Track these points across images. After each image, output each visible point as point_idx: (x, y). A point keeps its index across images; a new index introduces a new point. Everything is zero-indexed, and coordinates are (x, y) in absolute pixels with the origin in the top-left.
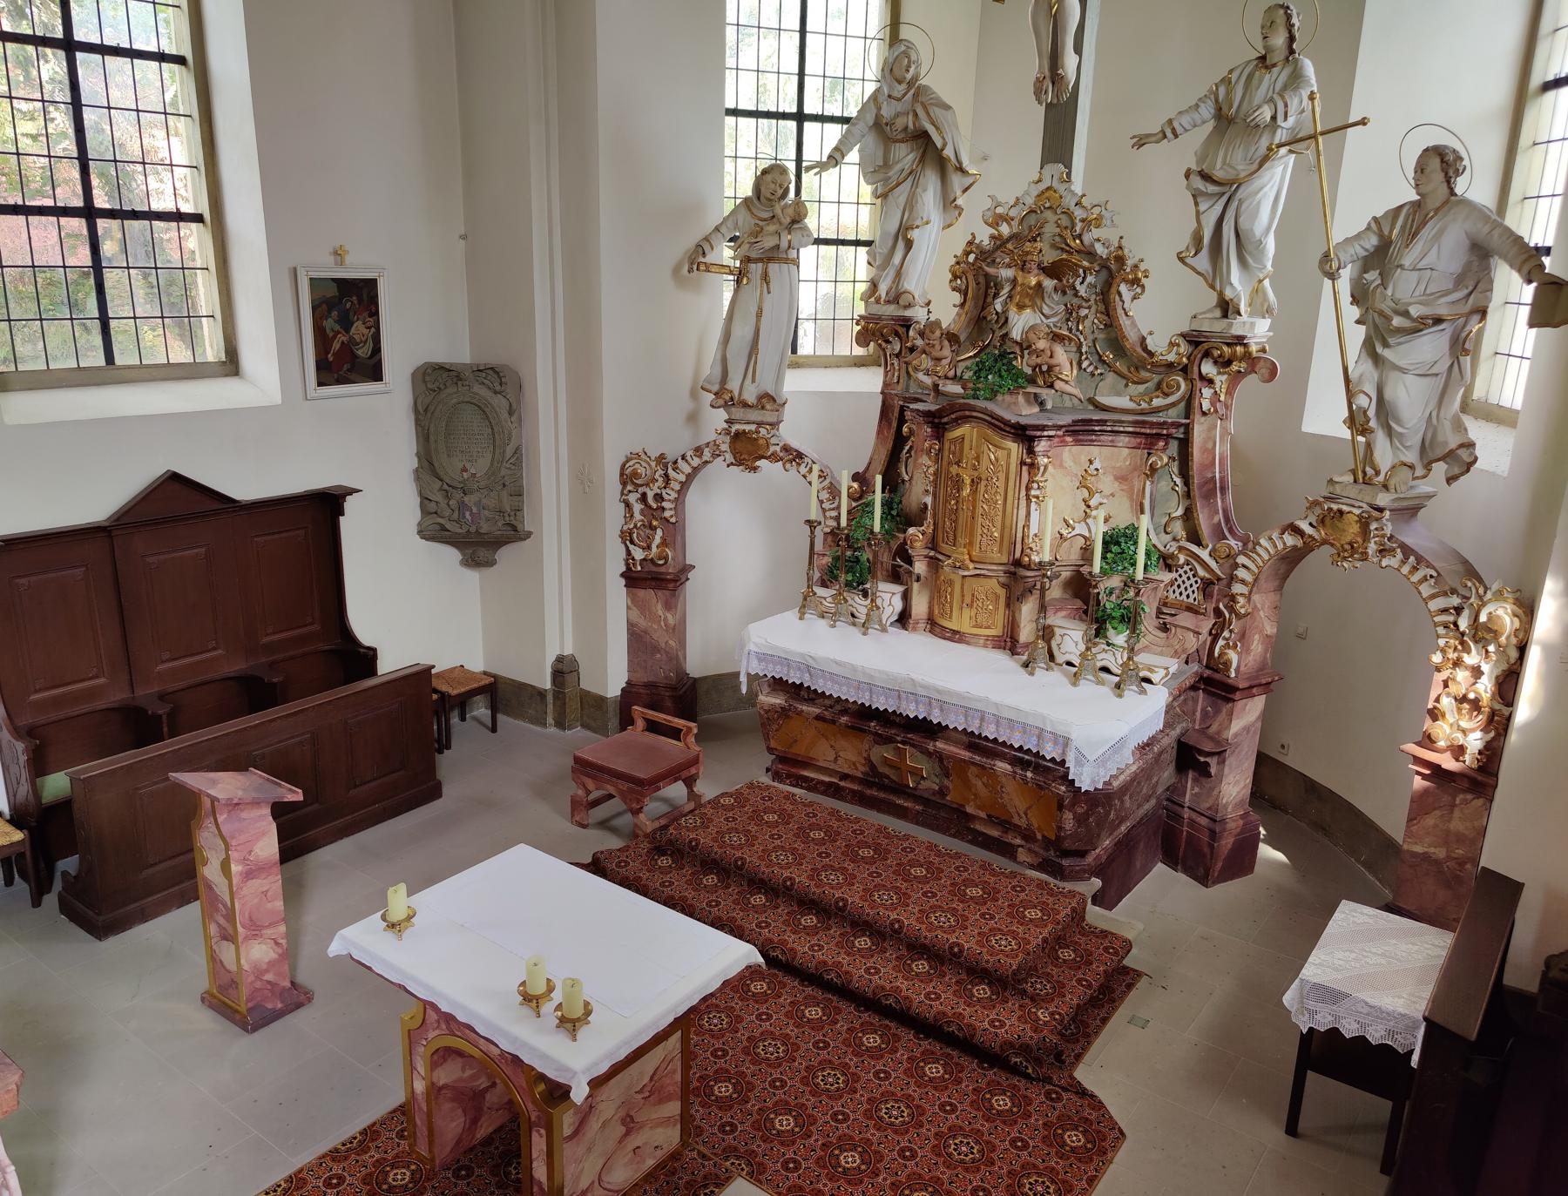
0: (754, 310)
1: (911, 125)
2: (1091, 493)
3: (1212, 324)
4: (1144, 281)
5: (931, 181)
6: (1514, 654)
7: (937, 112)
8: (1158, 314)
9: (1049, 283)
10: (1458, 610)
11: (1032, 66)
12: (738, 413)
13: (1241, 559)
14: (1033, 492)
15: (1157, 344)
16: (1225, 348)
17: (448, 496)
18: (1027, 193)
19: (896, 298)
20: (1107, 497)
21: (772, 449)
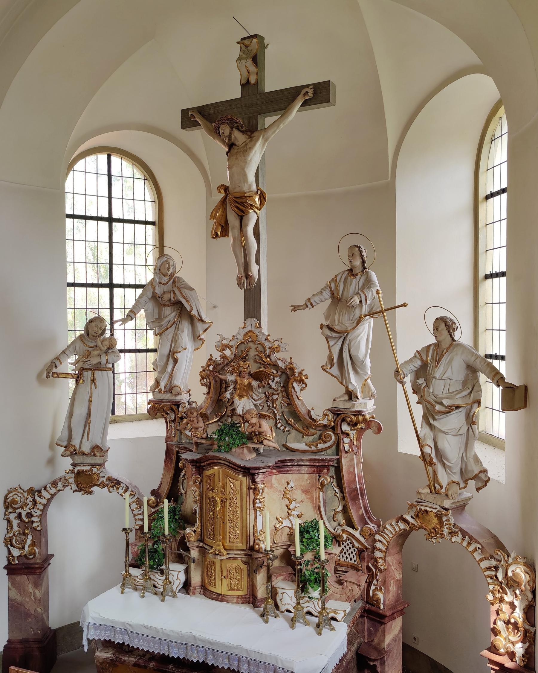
0: (87, 398)
1: (172, 299)
2: (290, 502)
3: (343, 405)
4: (306, 380)
5: (186, 327)
6: (530, 596)
7: (186, 292)
8: (316, 397)
9: (255, 383)
10: (496, 568)
11: (235, 271)
12: (79, 459)
13: (377, 537)
14: (257, 505)
16: (353, 417)
18: (238, 333)
19: (170, 389)
20: (299, 503)
21: (101, 480)
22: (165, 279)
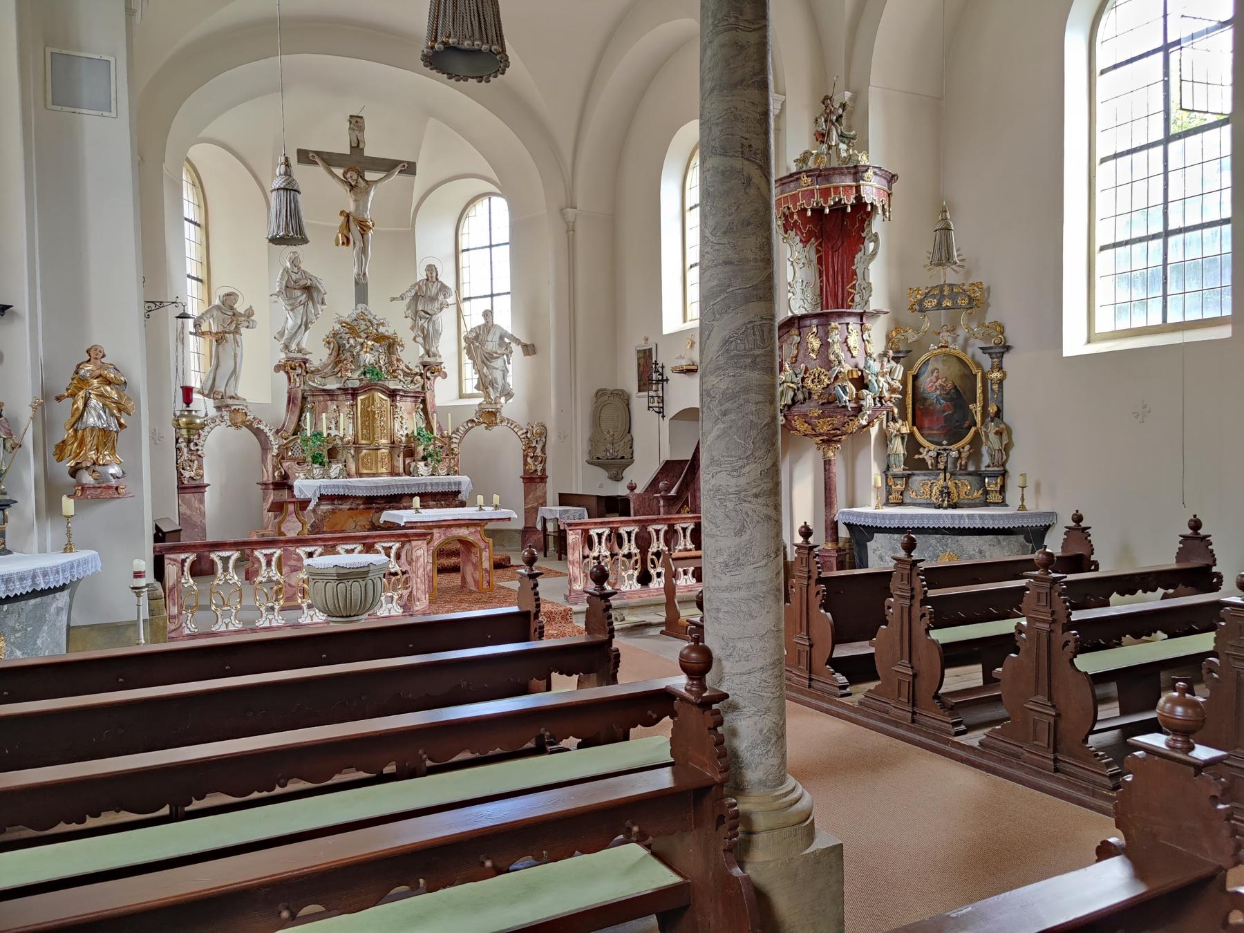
3: (426, 359)
8: (411, 355)
22: (296, 270)
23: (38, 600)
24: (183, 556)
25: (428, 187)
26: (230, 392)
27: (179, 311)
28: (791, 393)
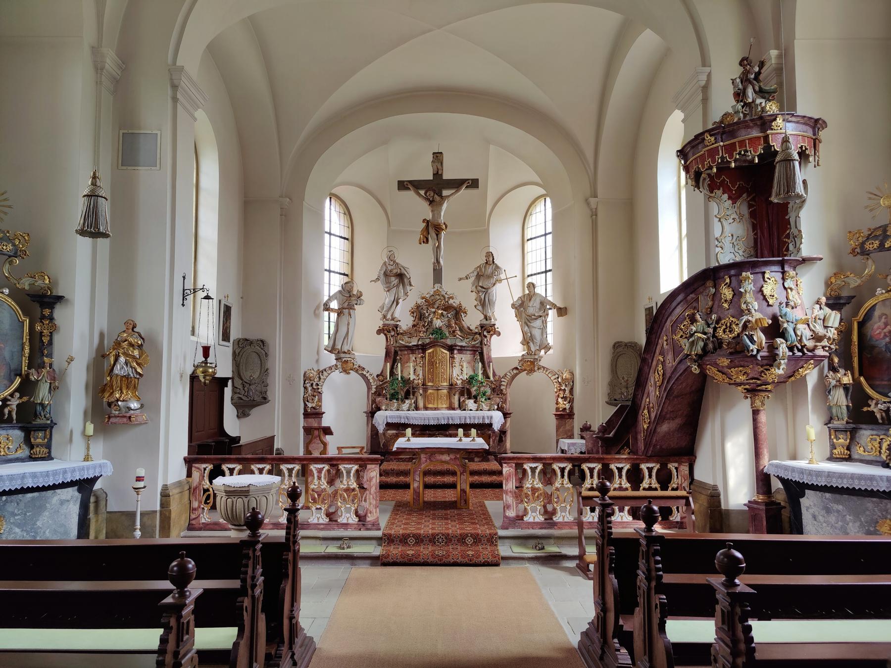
3: (485, 322)
8: (473, 320)
15: (473, 328)
17: (244, 387)
23: (36, 494)
24: (204, 466)
25: (498, 196)
26: (345, 349)
27: (205, 294)
28: (701, 344)
